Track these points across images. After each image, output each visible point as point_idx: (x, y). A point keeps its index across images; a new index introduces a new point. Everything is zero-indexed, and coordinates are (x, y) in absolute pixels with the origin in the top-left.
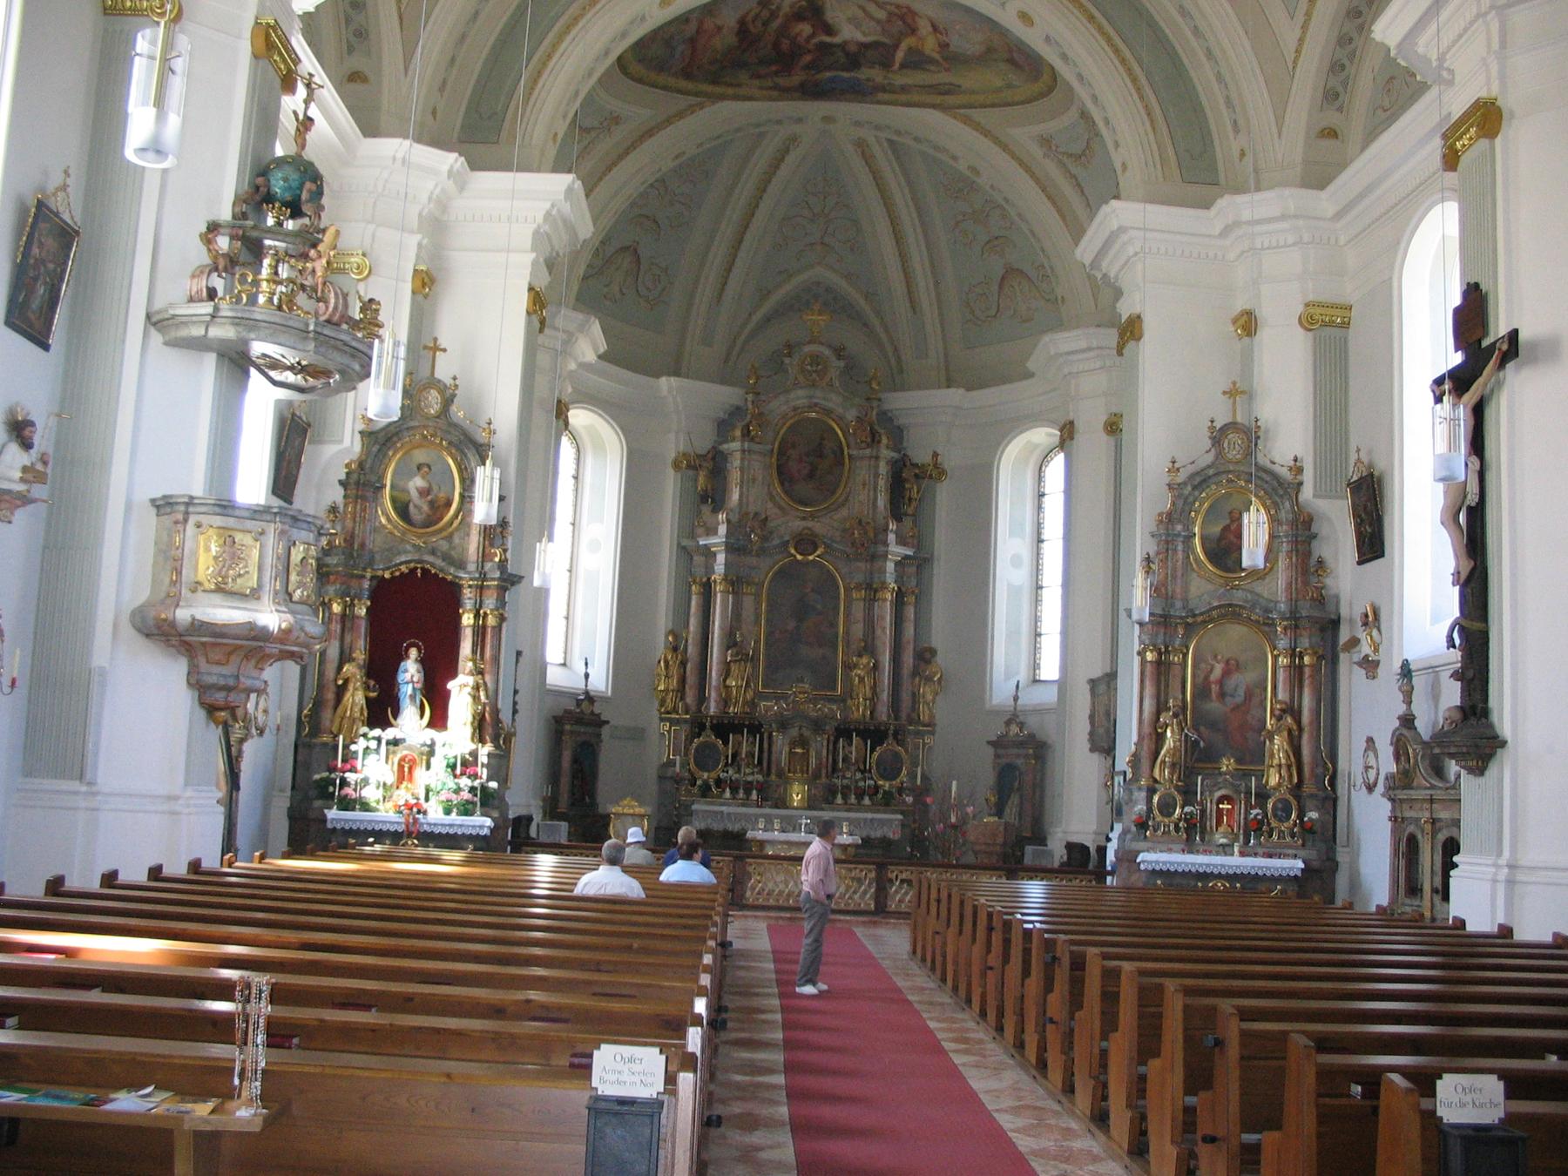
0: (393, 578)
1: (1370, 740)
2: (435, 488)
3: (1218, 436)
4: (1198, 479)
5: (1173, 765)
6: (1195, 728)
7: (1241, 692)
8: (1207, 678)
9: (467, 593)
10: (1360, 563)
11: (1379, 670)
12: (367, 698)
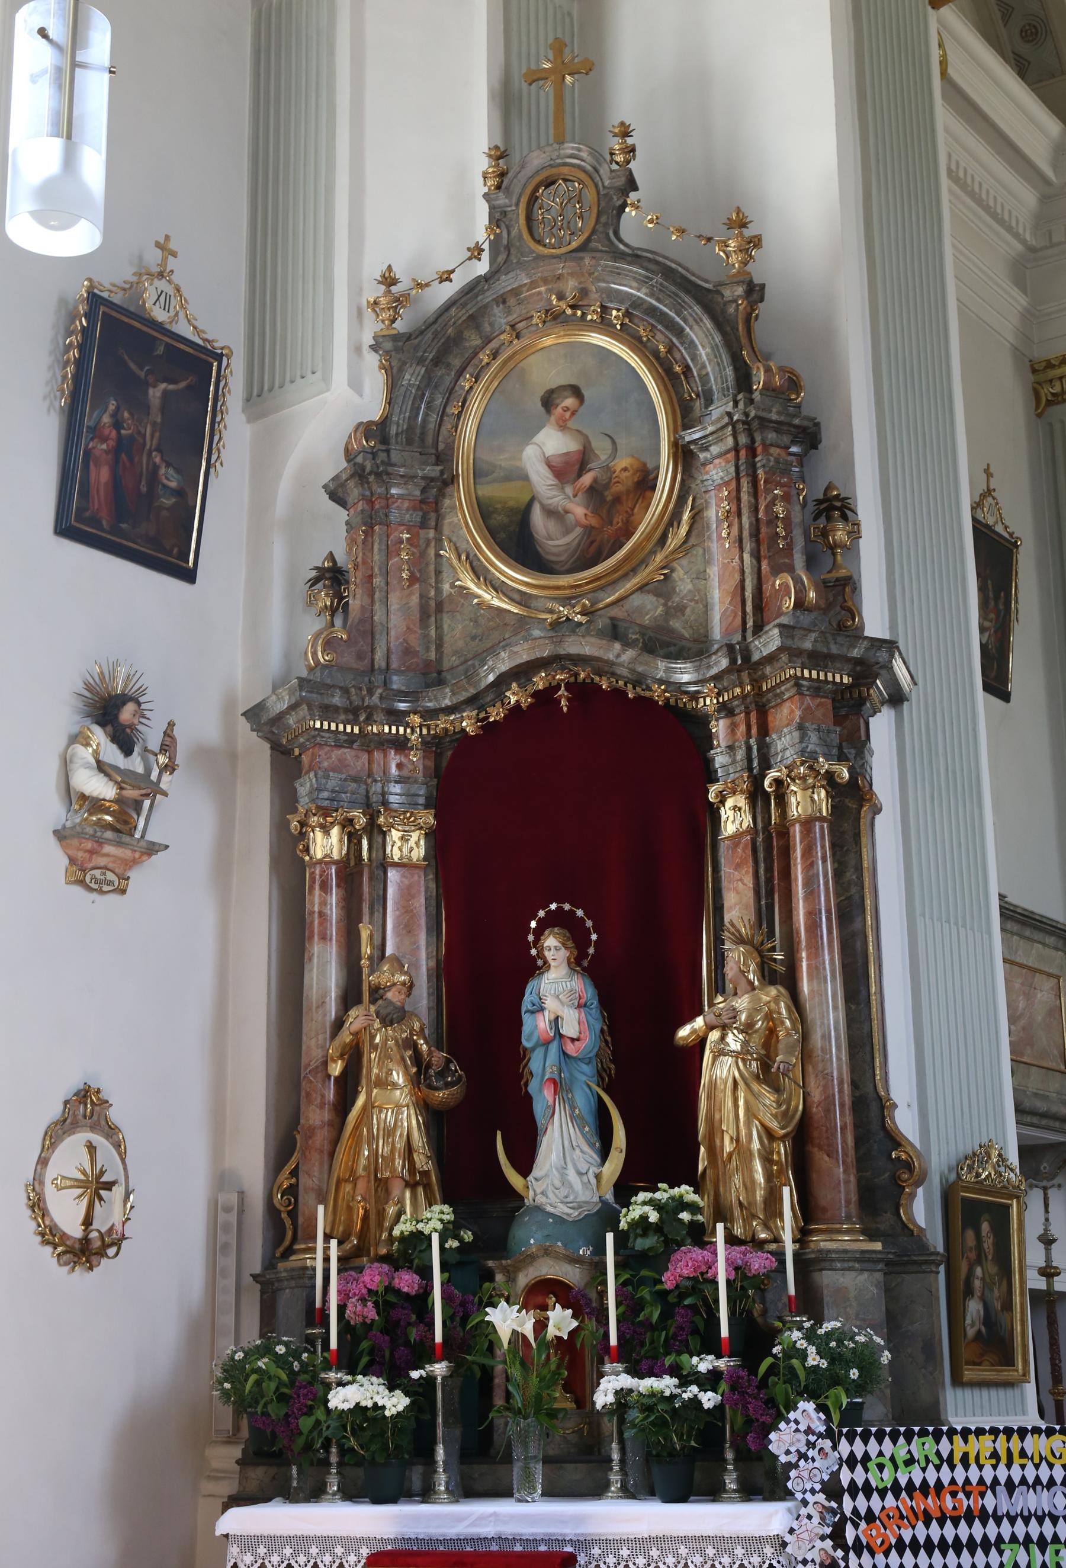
0: (488, 728)
2: (601, 448)
9: (719, 728)
12: (425, 1107)
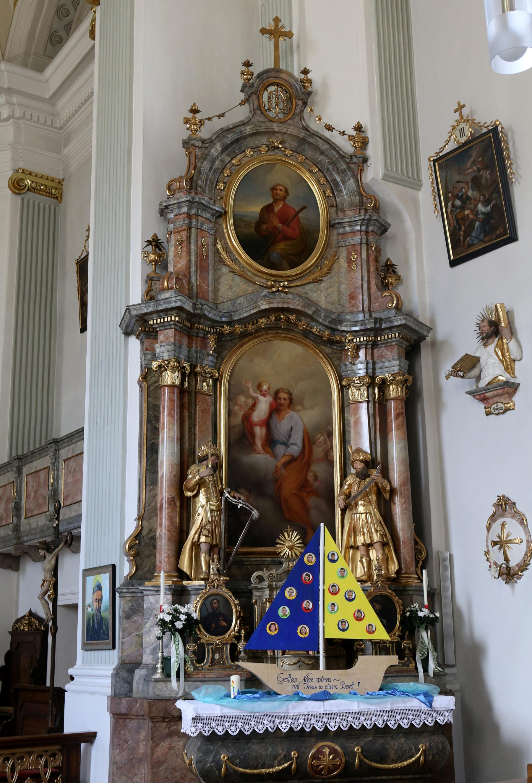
1: (504, 506)
3: (255, 85)
4: (230, 137)
5: (212, 548)
6: (233, 486)
7: (297, 438)
8: (247, 417)
10: (453, 263)
11: (516, 398)
